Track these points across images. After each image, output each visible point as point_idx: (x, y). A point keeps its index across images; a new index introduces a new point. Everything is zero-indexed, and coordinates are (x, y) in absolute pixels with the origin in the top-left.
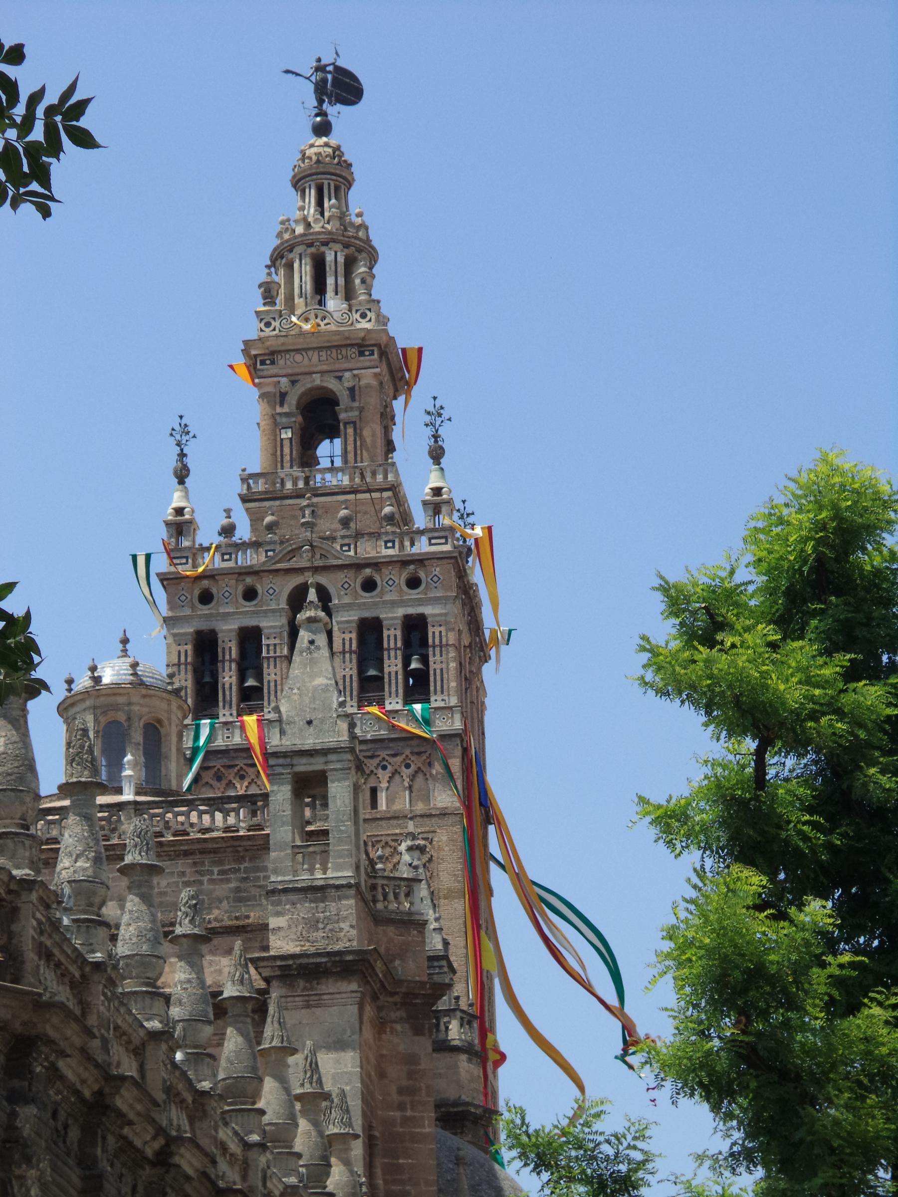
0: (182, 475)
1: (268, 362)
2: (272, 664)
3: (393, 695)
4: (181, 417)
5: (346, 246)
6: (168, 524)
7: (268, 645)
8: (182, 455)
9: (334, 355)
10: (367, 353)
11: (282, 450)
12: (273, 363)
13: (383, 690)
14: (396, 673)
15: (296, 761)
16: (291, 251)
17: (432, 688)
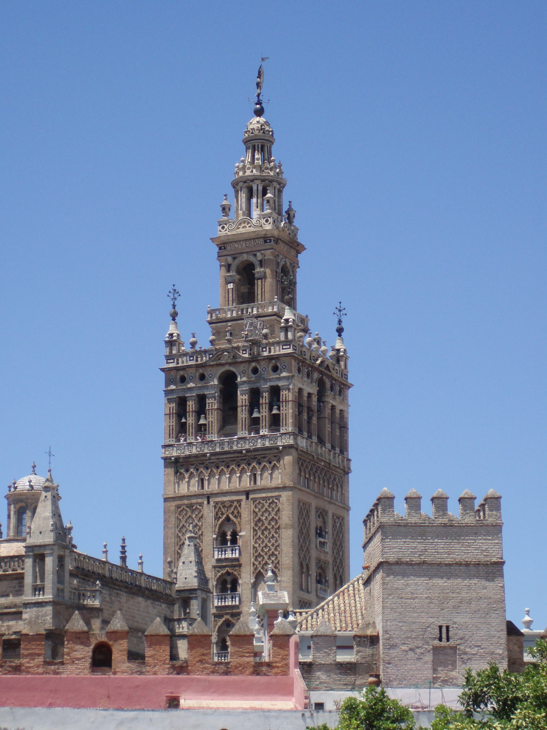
0: (174, 316)
1: (223, 248)
2: (210, 412)
3: (264, 427)
4: (174, 285)
5: (263, 181)
6: (166, 342)
7: (209, 403)
8: (174, 306)
9: (253, 243)
10: (268, 241)
11: (228, 295)
12: (225, 248)
13: (259, 424)
14: (265, 416)
15: (35, 549)
16: (237, 184)
17: (281, 423)
